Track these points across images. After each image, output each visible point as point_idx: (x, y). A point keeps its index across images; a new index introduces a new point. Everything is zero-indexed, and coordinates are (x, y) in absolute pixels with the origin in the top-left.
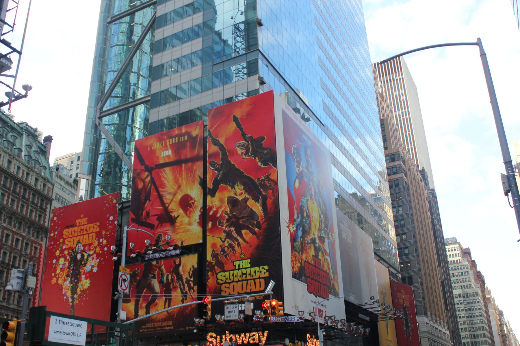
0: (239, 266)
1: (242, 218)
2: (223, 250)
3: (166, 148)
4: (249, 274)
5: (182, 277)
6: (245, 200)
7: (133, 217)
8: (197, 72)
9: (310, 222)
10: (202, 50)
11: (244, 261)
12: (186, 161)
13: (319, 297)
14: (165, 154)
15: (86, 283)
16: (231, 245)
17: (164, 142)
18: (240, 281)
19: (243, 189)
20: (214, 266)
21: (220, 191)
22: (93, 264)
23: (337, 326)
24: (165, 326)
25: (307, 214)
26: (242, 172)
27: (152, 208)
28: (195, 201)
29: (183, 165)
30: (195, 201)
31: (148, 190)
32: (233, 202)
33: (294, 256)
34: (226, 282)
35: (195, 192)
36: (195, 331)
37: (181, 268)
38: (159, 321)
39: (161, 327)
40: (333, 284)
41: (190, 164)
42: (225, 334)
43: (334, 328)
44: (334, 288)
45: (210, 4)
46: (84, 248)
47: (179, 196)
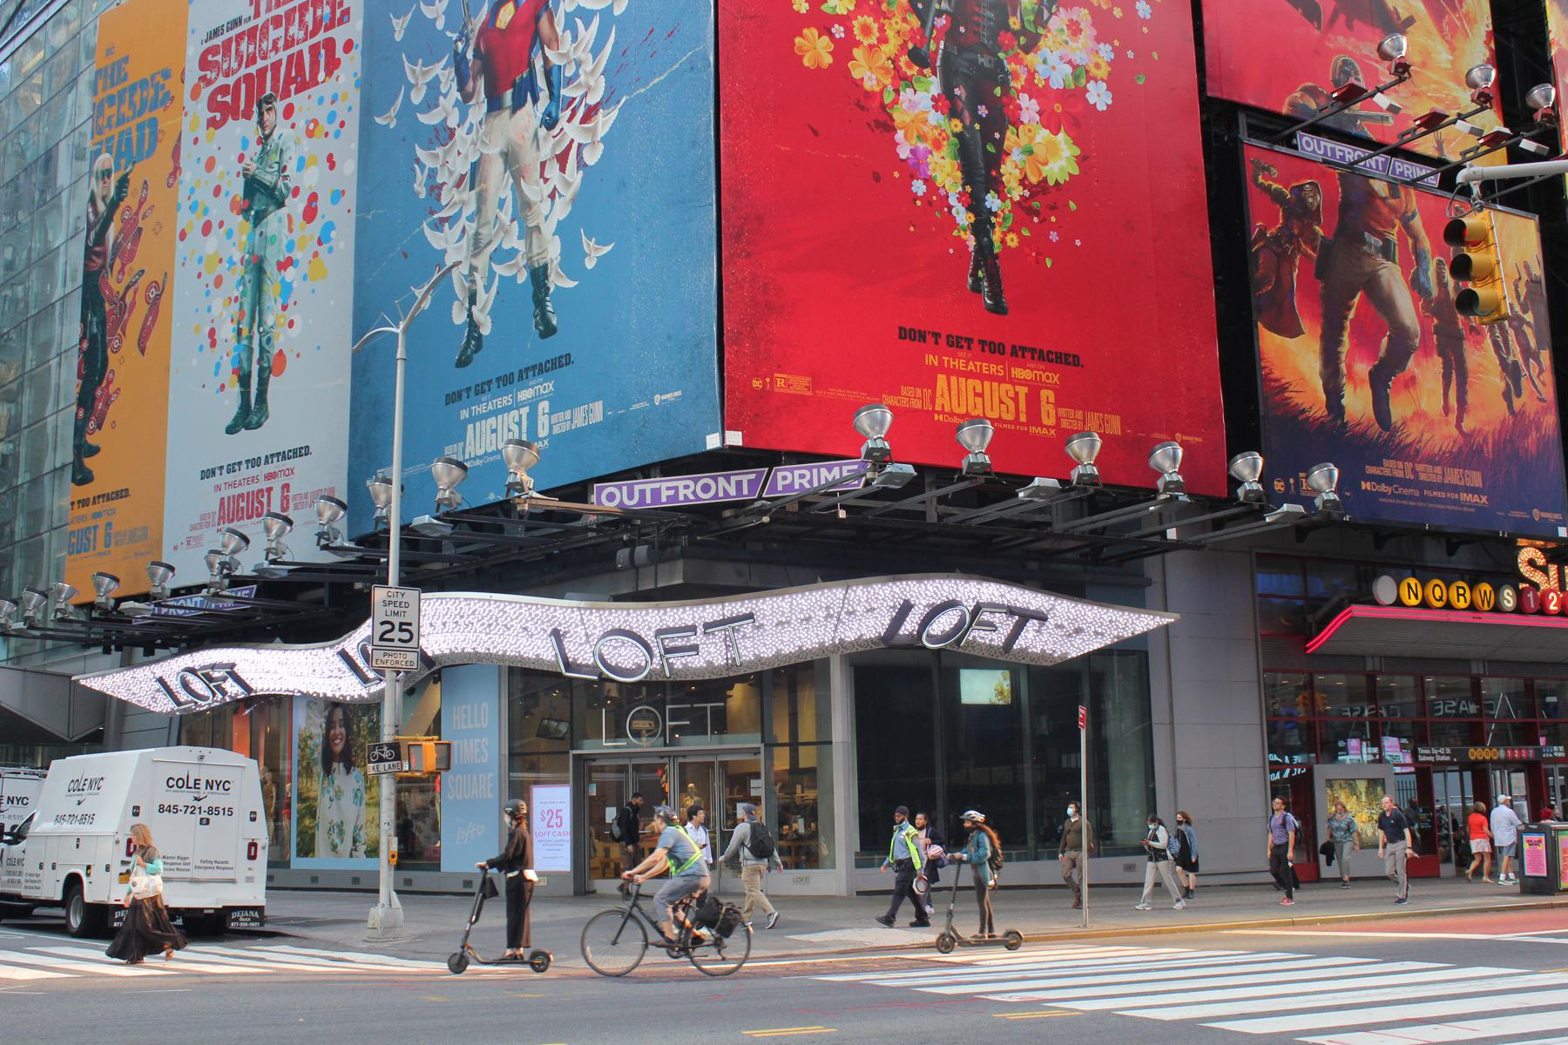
15: (1053, 150)
24: (1455, 488)
38: (1432, 460)
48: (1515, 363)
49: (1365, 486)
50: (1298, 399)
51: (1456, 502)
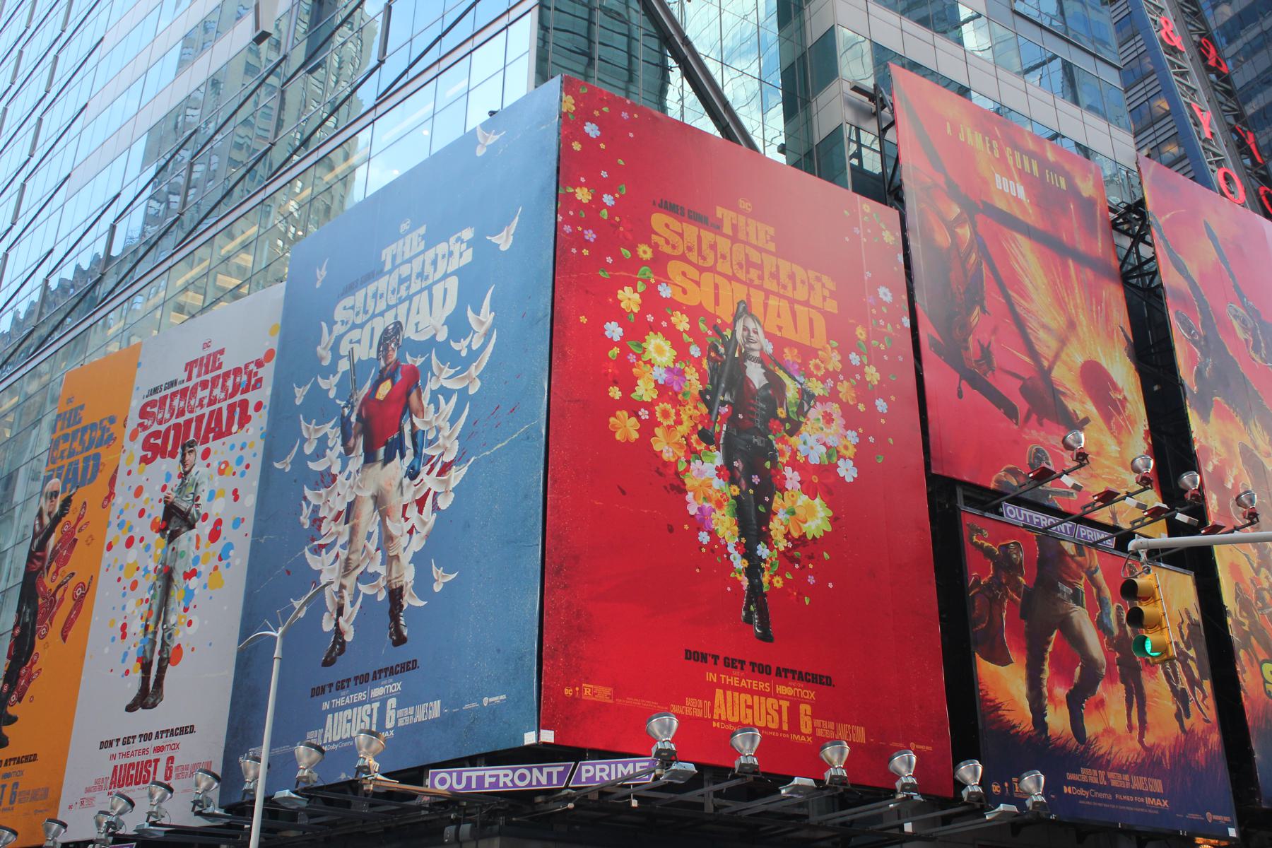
15: (811, 512)
24: (1141, 793)
38: (1121, 769)
48: (1183, 690)
50: (1010, 717)
51: (1143, 805)
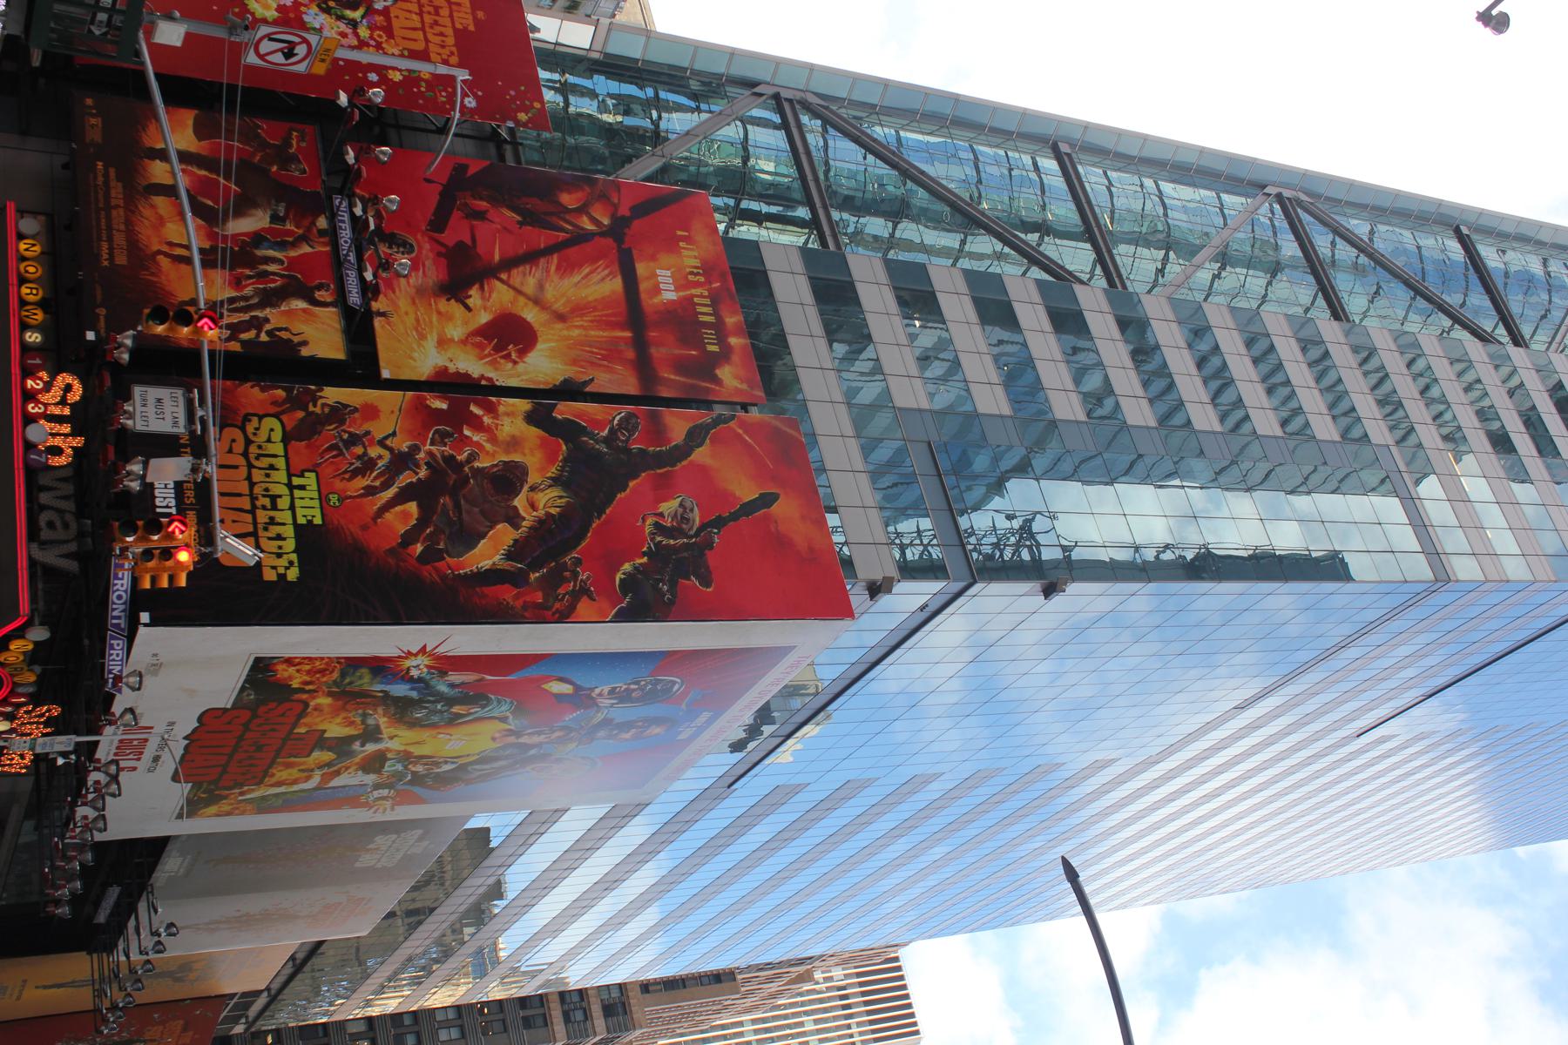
0: (302, 488)
1: (457, 506)
2: (354, 440)
3: (682, 283)
4: (272, 519)
5: (272, 305)
6: (514, 519)
7: (472, 171)
8: (911, 393)
9: (434, 726)
10: (975, 415)
11: (316, 503)
12: (640, 344)
13: (186, 748)
14: (664, 282)
16: (369, 464)
17: (702, 279)
18: (251, 489)
19: (548, 514)
20: (305, 409)
21: (541, 438)
22: (326, 33)
23: (85, 804)
24: (110, 239)
25: (459, 716)
26: (601, 512)
27: (497, 231)
28: (515, 363)
29: (628, 334)
30: (515, 363)
31: (554, 220)
32: (509, 479)
33: (330, 664)
34: (248, 442)
35: (542, 365)
36: (90, 336)
37: (300, 304)
39: (109, 228)
40: (226, 797)
41: (630, 354)
42: (73, 434)
43: (78, 795)
44: (213, 799)
45: (1109, 444)
46: (377, 11)
47: (531, 315)
49: (100, 165)
